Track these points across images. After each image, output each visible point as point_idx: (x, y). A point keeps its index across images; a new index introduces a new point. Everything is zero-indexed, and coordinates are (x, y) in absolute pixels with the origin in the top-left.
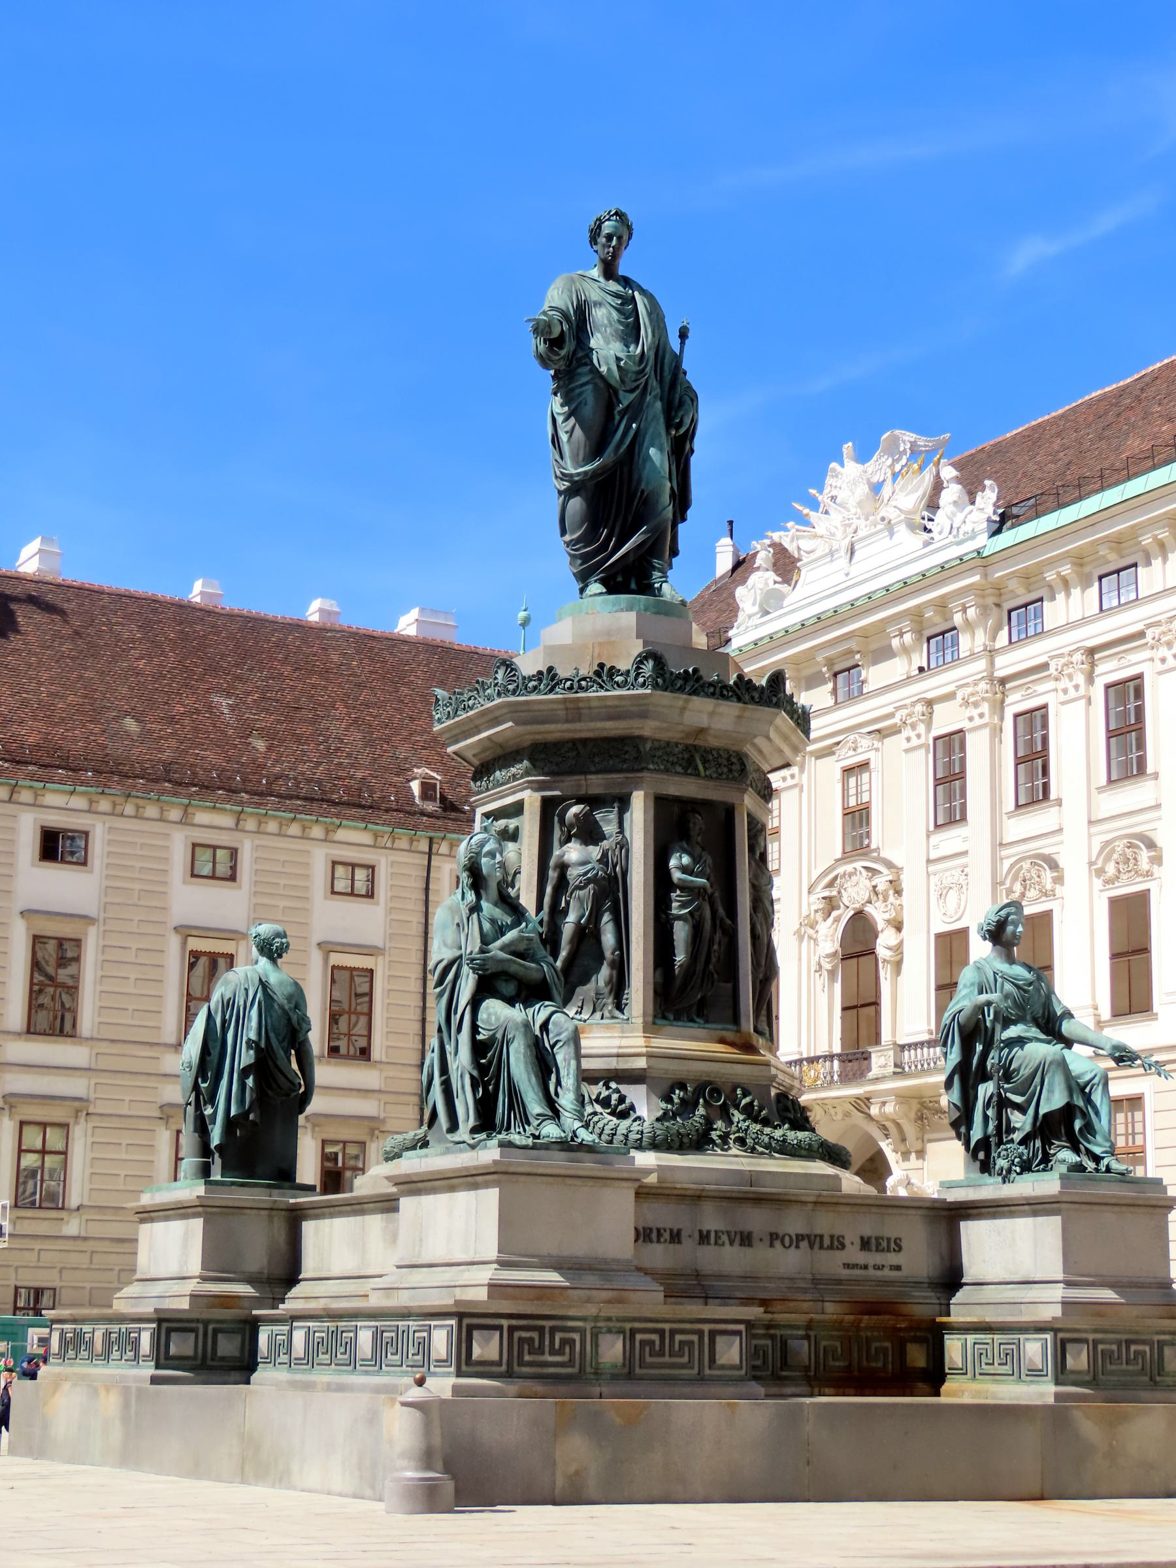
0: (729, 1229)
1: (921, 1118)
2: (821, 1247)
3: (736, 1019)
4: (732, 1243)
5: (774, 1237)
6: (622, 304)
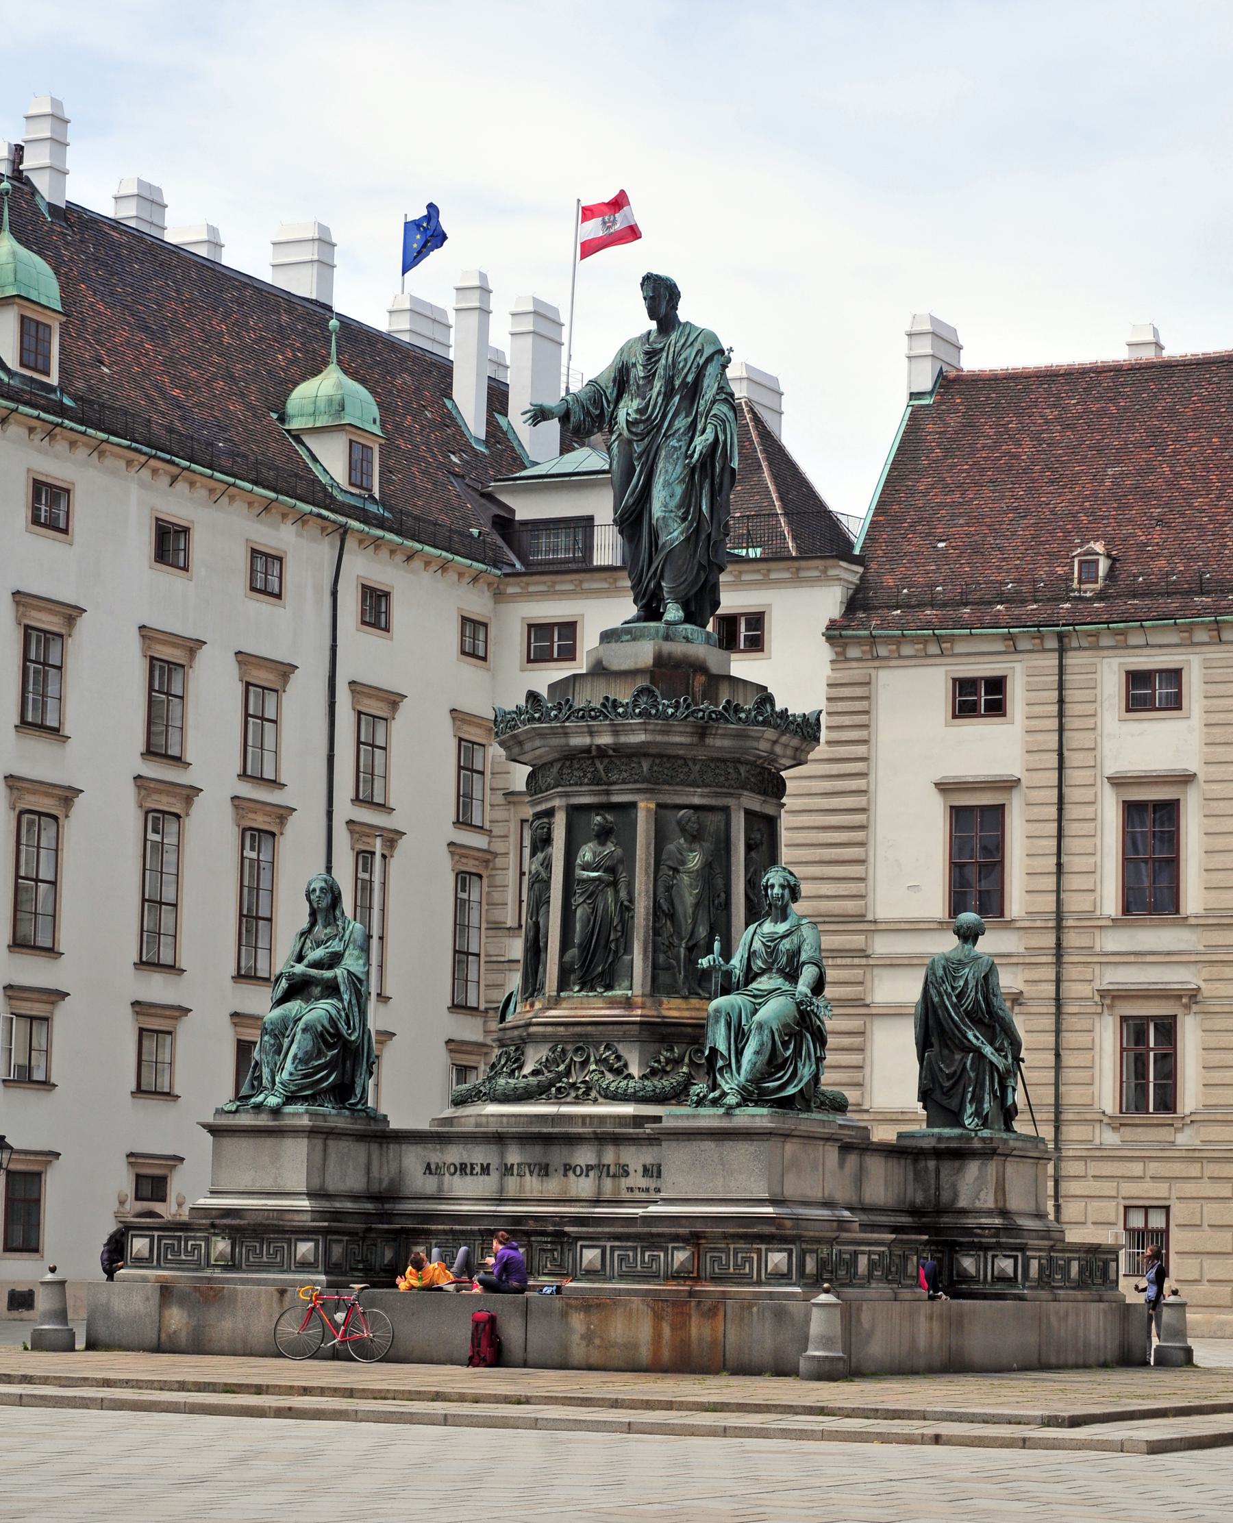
0: (530, 1161)
2: (608, 1175)
4: (531, 1173)
5: (568, 1168)
6: (649, 359)
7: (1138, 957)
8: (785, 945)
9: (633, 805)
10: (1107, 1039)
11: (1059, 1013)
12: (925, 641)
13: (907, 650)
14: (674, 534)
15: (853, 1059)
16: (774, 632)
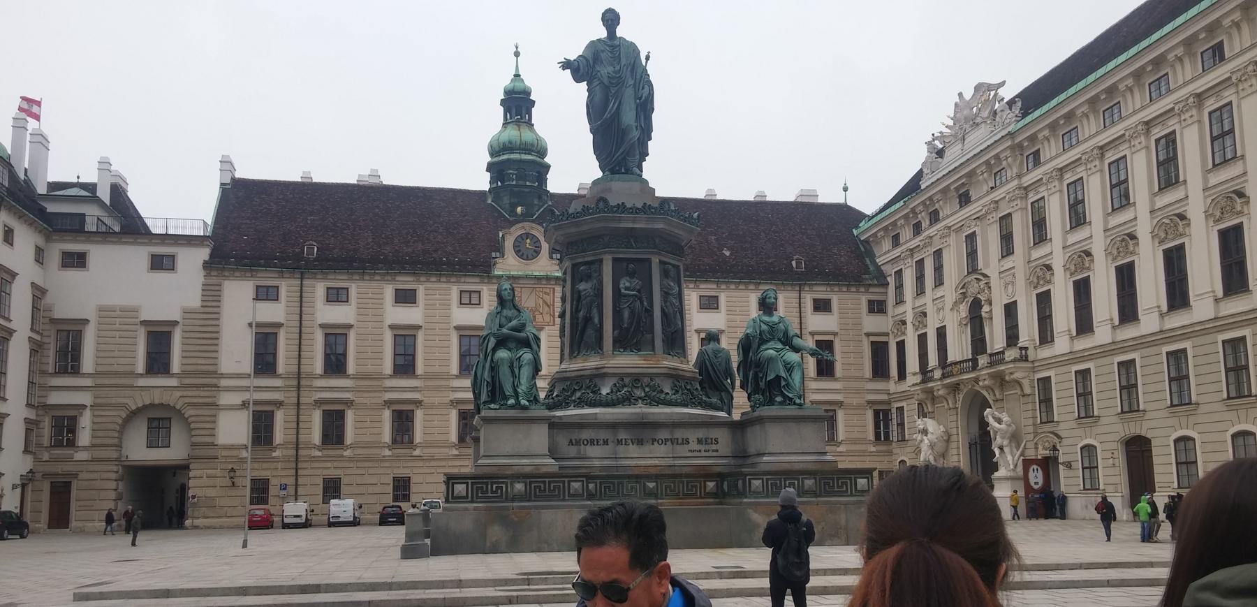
1: (1002, 385)
3: (653, 350)
5: (654, 440)
7: (331, 389)
8: (781, 326)
9: (649, 261)
10: (317, 418)
11: (298, 409)
12: (246, 271)
13: (237, 274)
14: (635, 134)
15: (211, 426)
16: (181, 263)
